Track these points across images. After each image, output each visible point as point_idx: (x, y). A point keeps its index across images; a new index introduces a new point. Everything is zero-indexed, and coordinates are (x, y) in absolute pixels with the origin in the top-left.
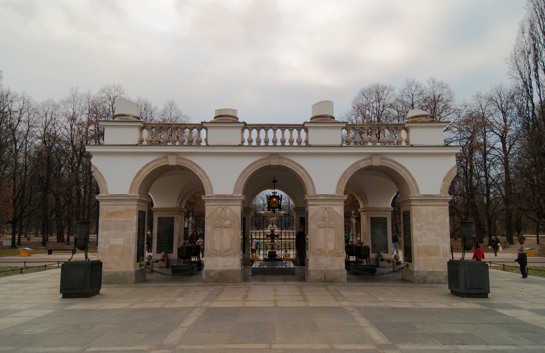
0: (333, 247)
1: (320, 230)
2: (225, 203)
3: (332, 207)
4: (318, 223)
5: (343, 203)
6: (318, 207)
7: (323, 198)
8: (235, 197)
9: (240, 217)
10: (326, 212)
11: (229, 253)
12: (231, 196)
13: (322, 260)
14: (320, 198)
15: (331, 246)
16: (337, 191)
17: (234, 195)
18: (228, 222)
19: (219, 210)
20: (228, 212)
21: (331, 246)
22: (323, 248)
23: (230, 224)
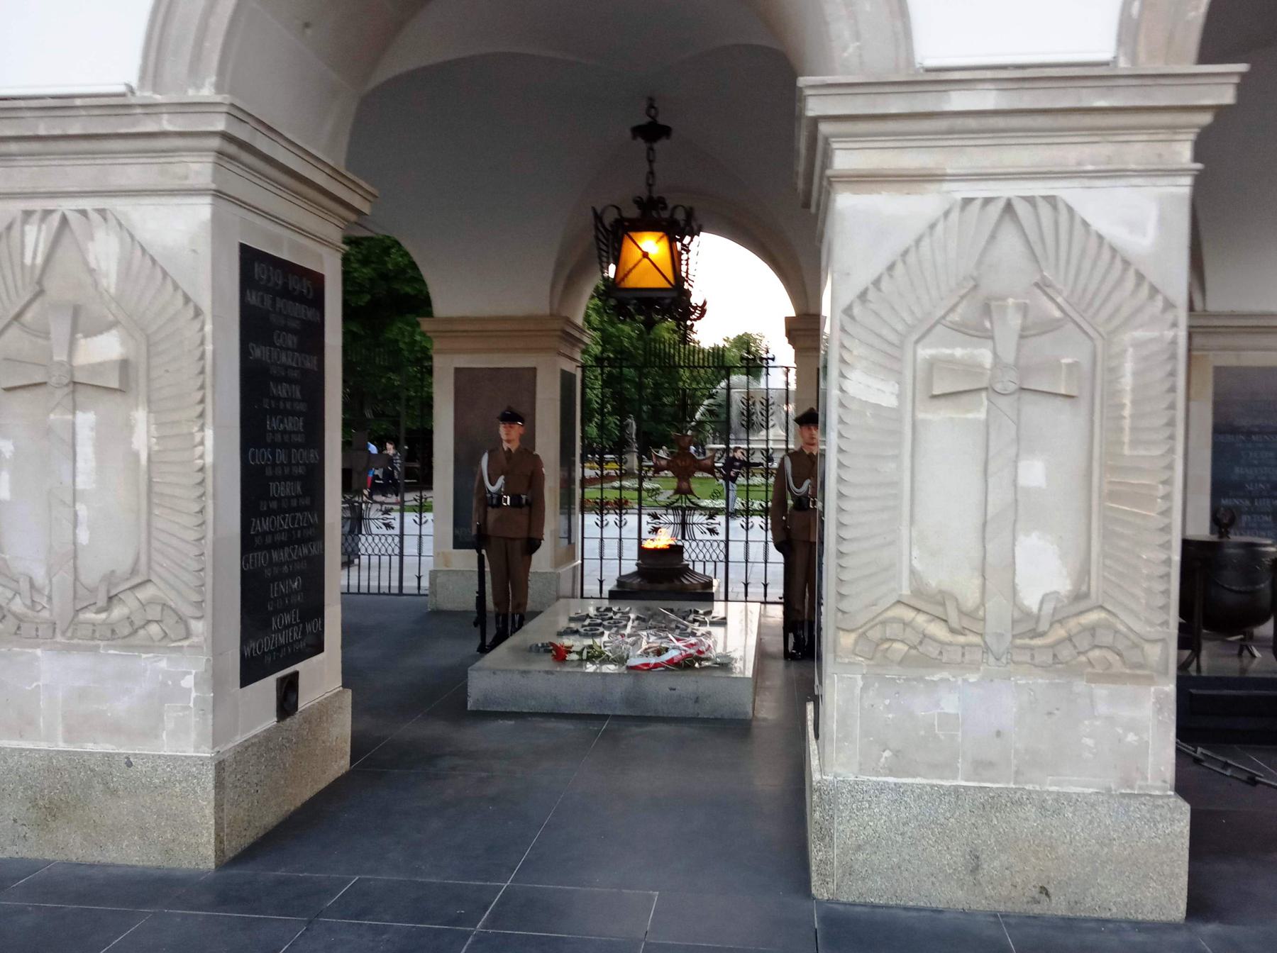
0: (1063, 585)
1: (937, 417)
2: (80, 173)
3: (1066, 191)
4: (925, 352)
5: (1183, 152)
6: (922, 206)
7: (987, 99)
8: (150, 108)
9: (206, 303)
10: (1010, 242)
11: (118, 612)
12: (115, 105)
13: (950, 704)
14: (959, 101)
15: (1042, 572)
16: (1128, 31)
17: (147, 95)
18: (105, 348)
19: (35, 239)
20: (104, 251)
21: (1042, 571)
22: (968, 589)
23: (124, 365)
